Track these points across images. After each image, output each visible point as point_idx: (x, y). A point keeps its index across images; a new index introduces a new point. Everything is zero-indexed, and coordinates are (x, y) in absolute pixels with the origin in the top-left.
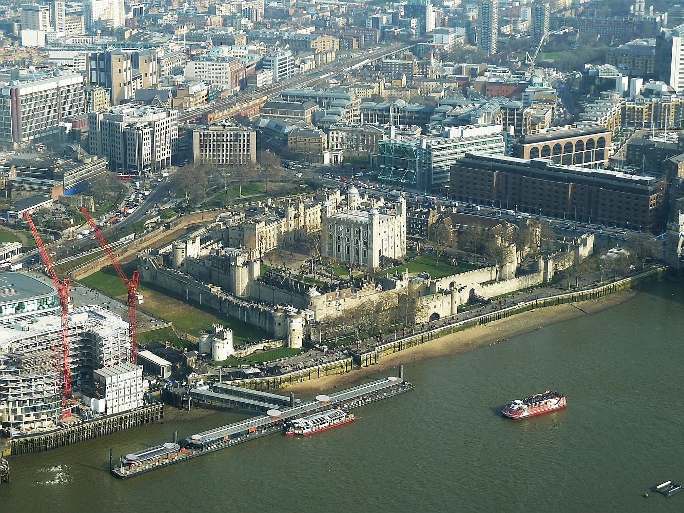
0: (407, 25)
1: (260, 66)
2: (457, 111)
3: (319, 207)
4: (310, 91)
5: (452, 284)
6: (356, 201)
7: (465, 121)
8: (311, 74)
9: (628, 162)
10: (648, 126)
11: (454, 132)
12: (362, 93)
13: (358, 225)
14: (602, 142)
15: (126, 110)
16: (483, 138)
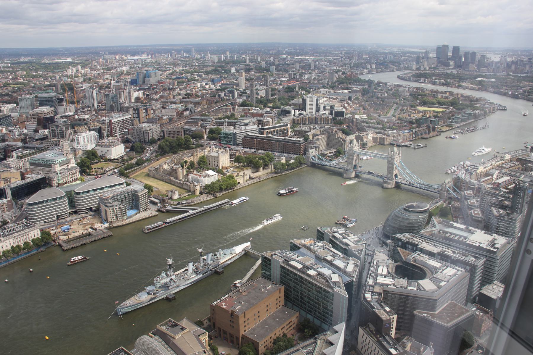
0: (229, 96)
1: (185, 110)
2: (244, 121)
3: (203, 152)
4: (199, 117)
5: (244, 173)
6: (214, 150)
7: (247, 124)
8: (200, 112)
9: (295, 135)
10: (300, 124)
11: (243, 128)
12: (215, 117)
13: (215, 157)
14: (287, 129)
15: (144, 125)
16: (251, 128)
